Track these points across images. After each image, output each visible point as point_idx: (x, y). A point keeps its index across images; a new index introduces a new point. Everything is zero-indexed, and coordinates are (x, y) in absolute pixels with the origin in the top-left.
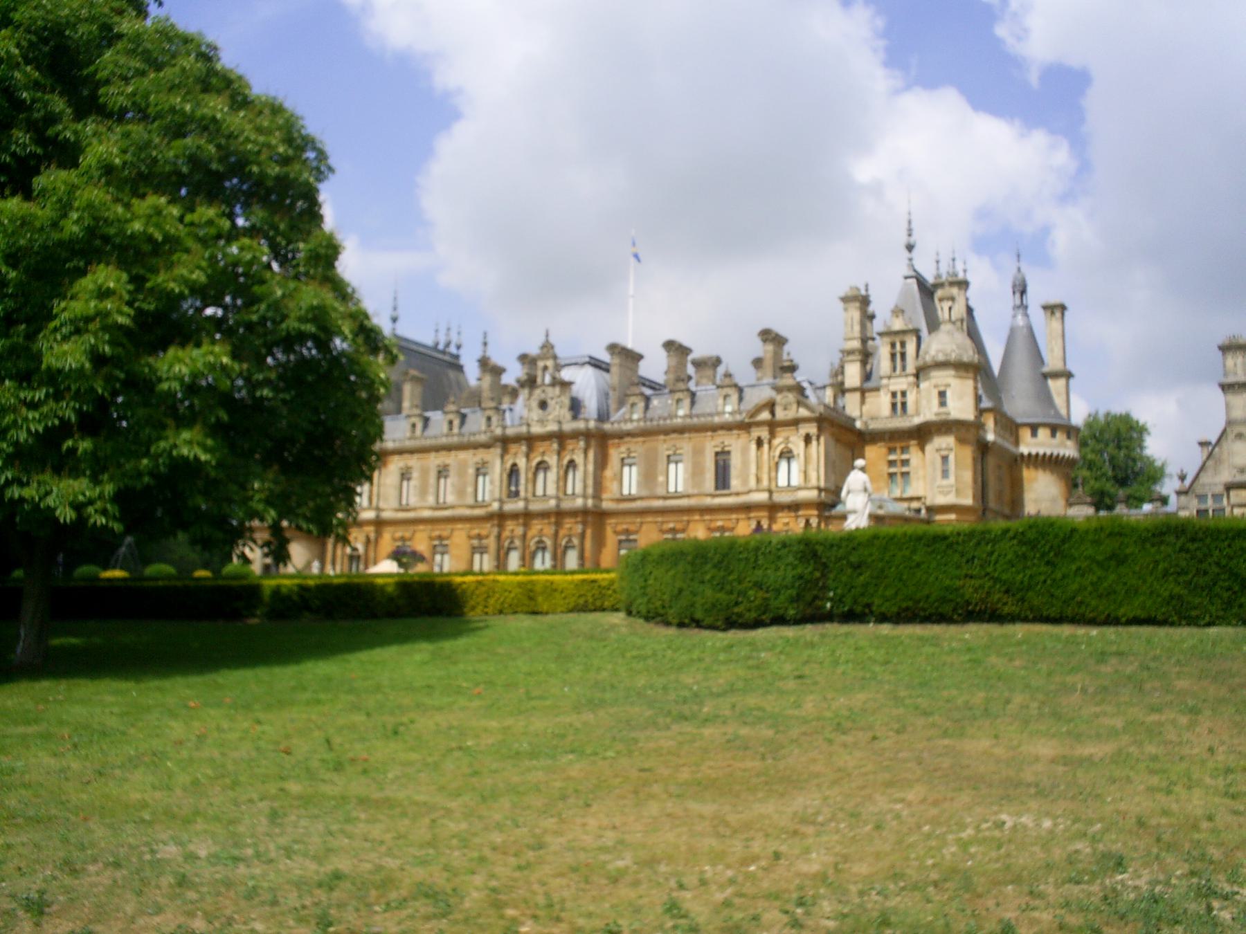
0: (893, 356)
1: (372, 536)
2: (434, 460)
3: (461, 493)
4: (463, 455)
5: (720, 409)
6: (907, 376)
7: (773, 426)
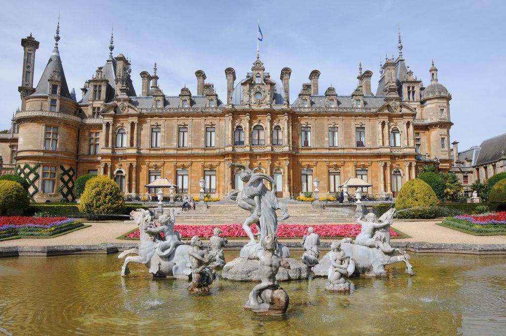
0: (409, 92)
1: (135, 164)
2: (175, 122)
3: (196, 140)
4: (196, 120)
5: (355, 106)
6: (417, 102)
7: (391, 117)
